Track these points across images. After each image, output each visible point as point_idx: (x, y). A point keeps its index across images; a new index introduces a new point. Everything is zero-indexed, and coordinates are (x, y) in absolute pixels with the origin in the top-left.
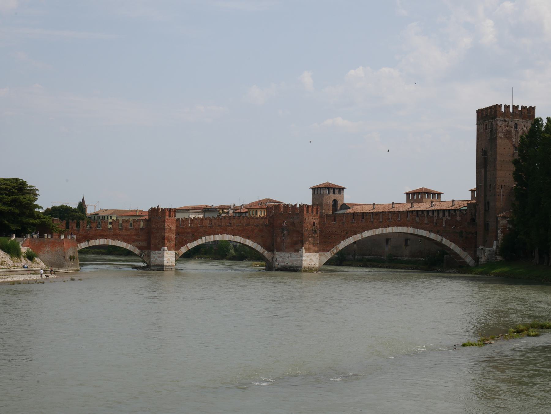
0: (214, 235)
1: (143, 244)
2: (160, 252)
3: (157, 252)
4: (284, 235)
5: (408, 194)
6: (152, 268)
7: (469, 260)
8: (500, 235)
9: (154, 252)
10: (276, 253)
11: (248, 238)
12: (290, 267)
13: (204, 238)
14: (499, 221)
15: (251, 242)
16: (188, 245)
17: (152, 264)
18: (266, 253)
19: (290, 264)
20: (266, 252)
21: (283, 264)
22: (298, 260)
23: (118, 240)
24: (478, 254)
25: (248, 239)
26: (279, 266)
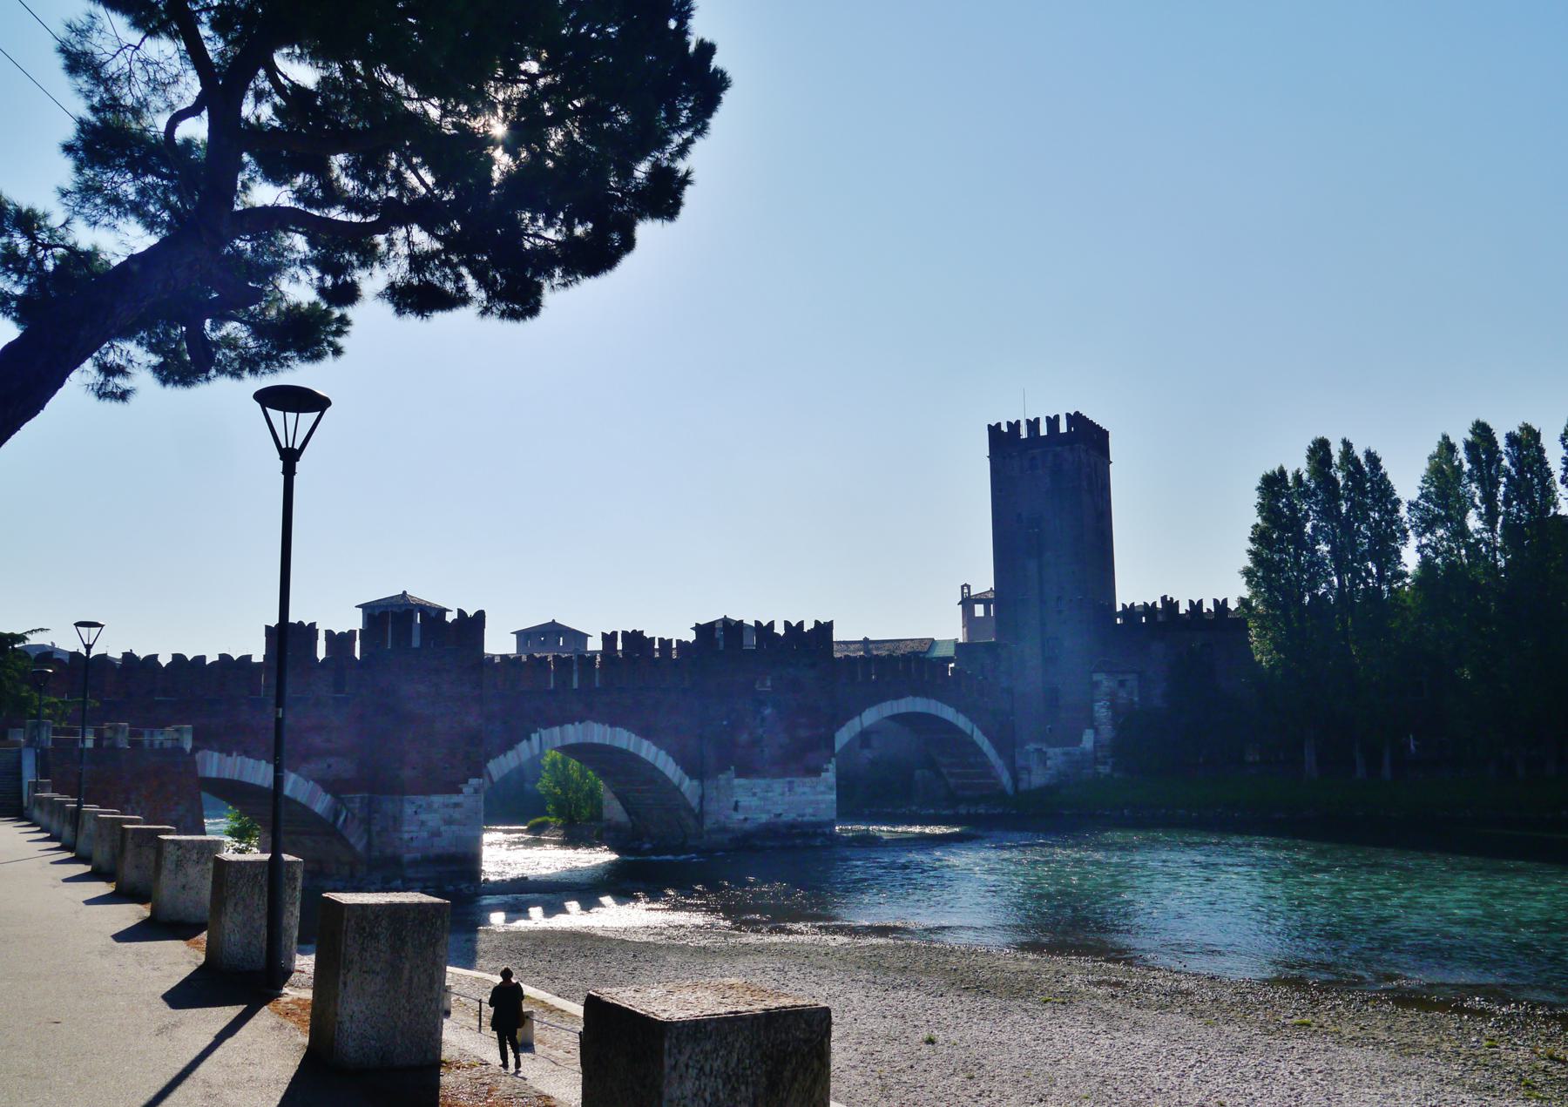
0: (561, 723)
1: (344, 768)
2: (455, 798)
3: (437, 800)
4: (763, 719)
5: (519, 634)
6: (410, 873)
7: (1006, 778)
8: (1102, 711)
9: (421, 800)
10: (737, 781)
11: (645, 732)
12: (792, 826)
13: (535, 737)
14: (1096, 685)
15: (654, 749)
16: (492, 766)
17: (407, 857)
18: (689, 786)
19: (789, 817)
20: (687, 782)
21: (764, 818)
22: (817, 803)
23: (247, 753)
24: (1020, 762)
25: (647, 737)
26: (747, 826)
